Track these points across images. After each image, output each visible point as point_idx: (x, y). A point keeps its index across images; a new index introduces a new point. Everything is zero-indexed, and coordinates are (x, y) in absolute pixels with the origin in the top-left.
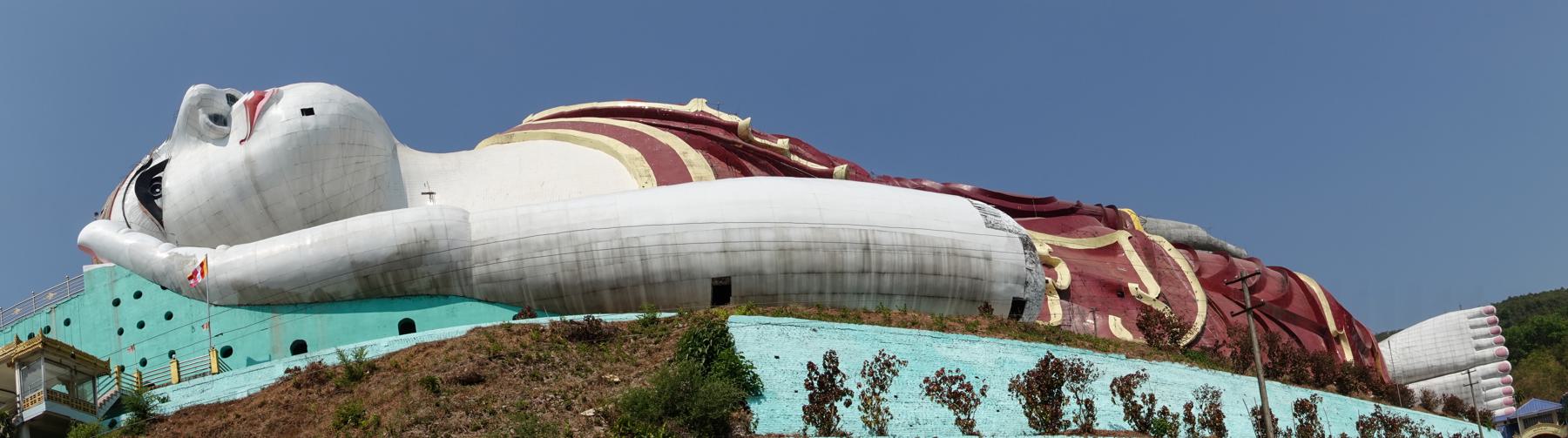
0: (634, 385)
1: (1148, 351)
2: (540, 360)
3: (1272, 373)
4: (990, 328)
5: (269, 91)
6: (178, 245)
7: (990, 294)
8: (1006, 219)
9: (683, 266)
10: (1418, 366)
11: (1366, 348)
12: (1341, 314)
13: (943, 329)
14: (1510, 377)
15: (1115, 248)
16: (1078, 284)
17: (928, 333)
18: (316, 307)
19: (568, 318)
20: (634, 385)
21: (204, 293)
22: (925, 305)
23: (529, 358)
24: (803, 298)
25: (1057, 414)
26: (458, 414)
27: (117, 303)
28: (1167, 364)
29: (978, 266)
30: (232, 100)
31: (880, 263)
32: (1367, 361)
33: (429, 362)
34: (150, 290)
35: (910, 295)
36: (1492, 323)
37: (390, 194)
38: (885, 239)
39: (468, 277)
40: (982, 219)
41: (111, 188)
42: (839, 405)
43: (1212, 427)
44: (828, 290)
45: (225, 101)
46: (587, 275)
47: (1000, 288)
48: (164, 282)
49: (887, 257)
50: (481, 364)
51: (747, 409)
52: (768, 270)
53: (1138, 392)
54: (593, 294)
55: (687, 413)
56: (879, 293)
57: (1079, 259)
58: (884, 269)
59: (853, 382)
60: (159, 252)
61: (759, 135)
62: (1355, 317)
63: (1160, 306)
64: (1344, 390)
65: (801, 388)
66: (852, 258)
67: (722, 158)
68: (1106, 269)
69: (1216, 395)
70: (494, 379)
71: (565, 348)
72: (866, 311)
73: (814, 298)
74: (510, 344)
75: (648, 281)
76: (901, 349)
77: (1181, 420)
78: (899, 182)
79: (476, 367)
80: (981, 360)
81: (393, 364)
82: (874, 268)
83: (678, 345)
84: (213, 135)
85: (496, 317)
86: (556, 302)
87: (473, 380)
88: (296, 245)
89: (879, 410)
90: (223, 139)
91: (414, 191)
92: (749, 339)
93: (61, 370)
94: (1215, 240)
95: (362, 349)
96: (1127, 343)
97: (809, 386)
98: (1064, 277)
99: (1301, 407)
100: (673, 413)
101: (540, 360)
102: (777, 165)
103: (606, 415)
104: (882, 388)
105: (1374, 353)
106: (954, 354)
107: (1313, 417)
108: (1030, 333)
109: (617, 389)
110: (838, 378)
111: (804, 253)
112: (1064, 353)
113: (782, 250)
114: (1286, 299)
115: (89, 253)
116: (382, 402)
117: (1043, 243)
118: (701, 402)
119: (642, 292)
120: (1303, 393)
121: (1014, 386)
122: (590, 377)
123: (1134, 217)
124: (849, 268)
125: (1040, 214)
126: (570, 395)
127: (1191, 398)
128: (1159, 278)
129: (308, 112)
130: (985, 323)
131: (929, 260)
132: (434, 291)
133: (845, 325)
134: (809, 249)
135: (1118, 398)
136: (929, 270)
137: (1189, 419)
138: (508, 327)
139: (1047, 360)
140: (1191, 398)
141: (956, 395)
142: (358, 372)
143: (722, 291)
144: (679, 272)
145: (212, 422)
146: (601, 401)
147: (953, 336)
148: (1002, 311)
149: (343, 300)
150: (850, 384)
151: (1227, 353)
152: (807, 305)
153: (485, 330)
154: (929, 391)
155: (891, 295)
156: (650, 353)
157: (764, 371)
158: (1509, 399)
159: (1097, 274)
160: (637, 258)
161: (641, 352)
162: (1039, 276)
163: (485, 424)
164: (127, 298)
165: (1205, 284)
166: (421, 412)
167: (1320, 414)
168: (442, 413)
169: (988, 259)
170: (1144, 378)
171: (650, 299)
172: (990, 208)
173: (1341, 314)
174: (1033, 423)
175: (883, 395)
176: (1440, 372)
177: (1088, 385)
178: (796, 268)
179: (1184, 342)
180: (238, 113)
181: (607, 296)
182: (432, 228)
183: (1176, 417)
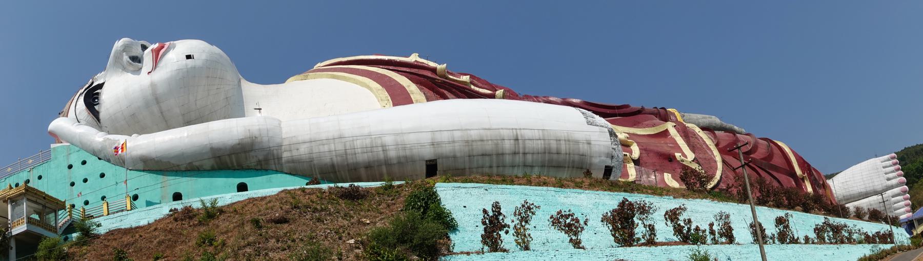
0: (379, 225)
1: (686, 193)
2: (322, 210)
3: (762, 202)
4: (590, 185)
5: (168, 43)
6: (109, 133)
7: (591, 164)
8: (599, 119)
9: (408, 153)
10: (852, 193)
11: (820, 183)
12: (804, 164)
13: (562, 186)
14: (908, 195)
15: (666, 133)
16: (644, 155)
17: (553, 189)
18: (189, 173)
19: (340, 185)
20: (379, 225)
21: (124, 162)
22: (552, 172)
23: (316, 209)
24: (480, 170)
25: (632, 234)
26: (274, 240)
27: (70, 167)
28: (698, 200)
29: (583, 148)
30: (144, 48)
31: (524, 148)
32: (821, 191)
33: (255, 209)
34: (91, 160)
35: (543, 166)
36: (895, 164)
37: (234, 108)
38: (528, 134)
39: (279, 158)
40: (584, 120)
41: (69, 97)
42: (502, 233)
43: (726, 236)
44: (494, 165)
45: (140, 48)
46: (351, 160)
47: (596, 160)
48: (100, 155)
49: (530, 145)
50: (287, 212)
51: (448, 238)
52: (458, 155)
53: (681, 218)
54: (355, 171)
55: (411, 241)
56: (525, 166)
57: (645, 140)
58: (527, 151)
59: (510, 219)
60: (98, 138)
61: (451, 74)
62: (813, 165)
63: (695, 166)
64: (807, 210)
65: (480, 224)
66: (508, 146)
67: (431, 89)
68: (662, 146)
69: (728, 216)
70: (295, 220)
71: (338, 203)
72: (517, 177)
73: (487, 170)
74: (304, 200)
75: (387, 163)
76: (537, 198)
77: (707, 233)
78: (536, 99)
79: (286, 211)
80: (585, 204)
81: (234, 209)
82: (521, 151)
83: (405, 201)
84: (131, 68)
85: (297, 183)
86: (332, 175)
87: (282, 221)
88: (178, 136)
89: (525, 235)
90: (138, 71)
91: (249, 106)
92: (448, 196)
93: (35, 206)
94: (725, 124)
95: (216, 200)
96: (675, 189)
97: (484, 223)
98: (636, 152)
99: (780, 221)
100: (401, 240)
101: (322, 210)
102: (463, 92)
103: (362, 243)
104: (526, 222)
105: (825, 186)
106: (568, 201)
107: (787, 227)
108: (614, 187)
109: (368, 227)
110: (501, 218)
111: (479, 143)
112: (634, 198)
113: (467, 141)
114: (770, 156)
115: (55, 137)
116: (226, 232)
117: (622, 132)
118: (420, 234)
120: (781, 213)
121: (605, 219)
122: (352, 221)
123: (677, 113)
124: (507, 152)
125: (620, 115)
126: (341, 231)
127: (713, 220)
128: (693, 148)
129: (189, 57)
130: (587, 181)
131: (554, 145)
132: (259, 167)
133: (504, 186)
134: (482, 140)
135: (669, 223)
137: (712, 232)
138: (303, 190)
139: (623, 202)
140: (713, 220)
141: (569, 225)
142: (212, 213)
143: (432, 168)
144: (406, 157)
145: (127, 239)
146: (359, 235)
147: (568, 190)
148: (598, 174)
149: (205, 170)
150: (507, 221)
151: (734, 191)
152: (483, 175)
153: (289, 192)
154: (553, 223)
155: (532, 166)
156: (388, 206)
157: (458, 215)
158: (908, 208)
159: (655, 149)
160: (380, 149)
161: (383, 205)
162: (620, 152)
163: (289, 247)
164: (77, 164)
165: (721, 151)
166: (251, 239)
167: (791, 224)
168: (264, 239)
169: (589, 143)
170: (685, 209)
171: (389, 174)
172: (590, 113)
173: (804, 164)
174: (617, 240)
175: (527, 226)
176: (866, 195)
177: (650, 216)
178: (475, 153)
179: (709, 187)
180: (148, 56)
181: (363, 172)
183: (704, 231)
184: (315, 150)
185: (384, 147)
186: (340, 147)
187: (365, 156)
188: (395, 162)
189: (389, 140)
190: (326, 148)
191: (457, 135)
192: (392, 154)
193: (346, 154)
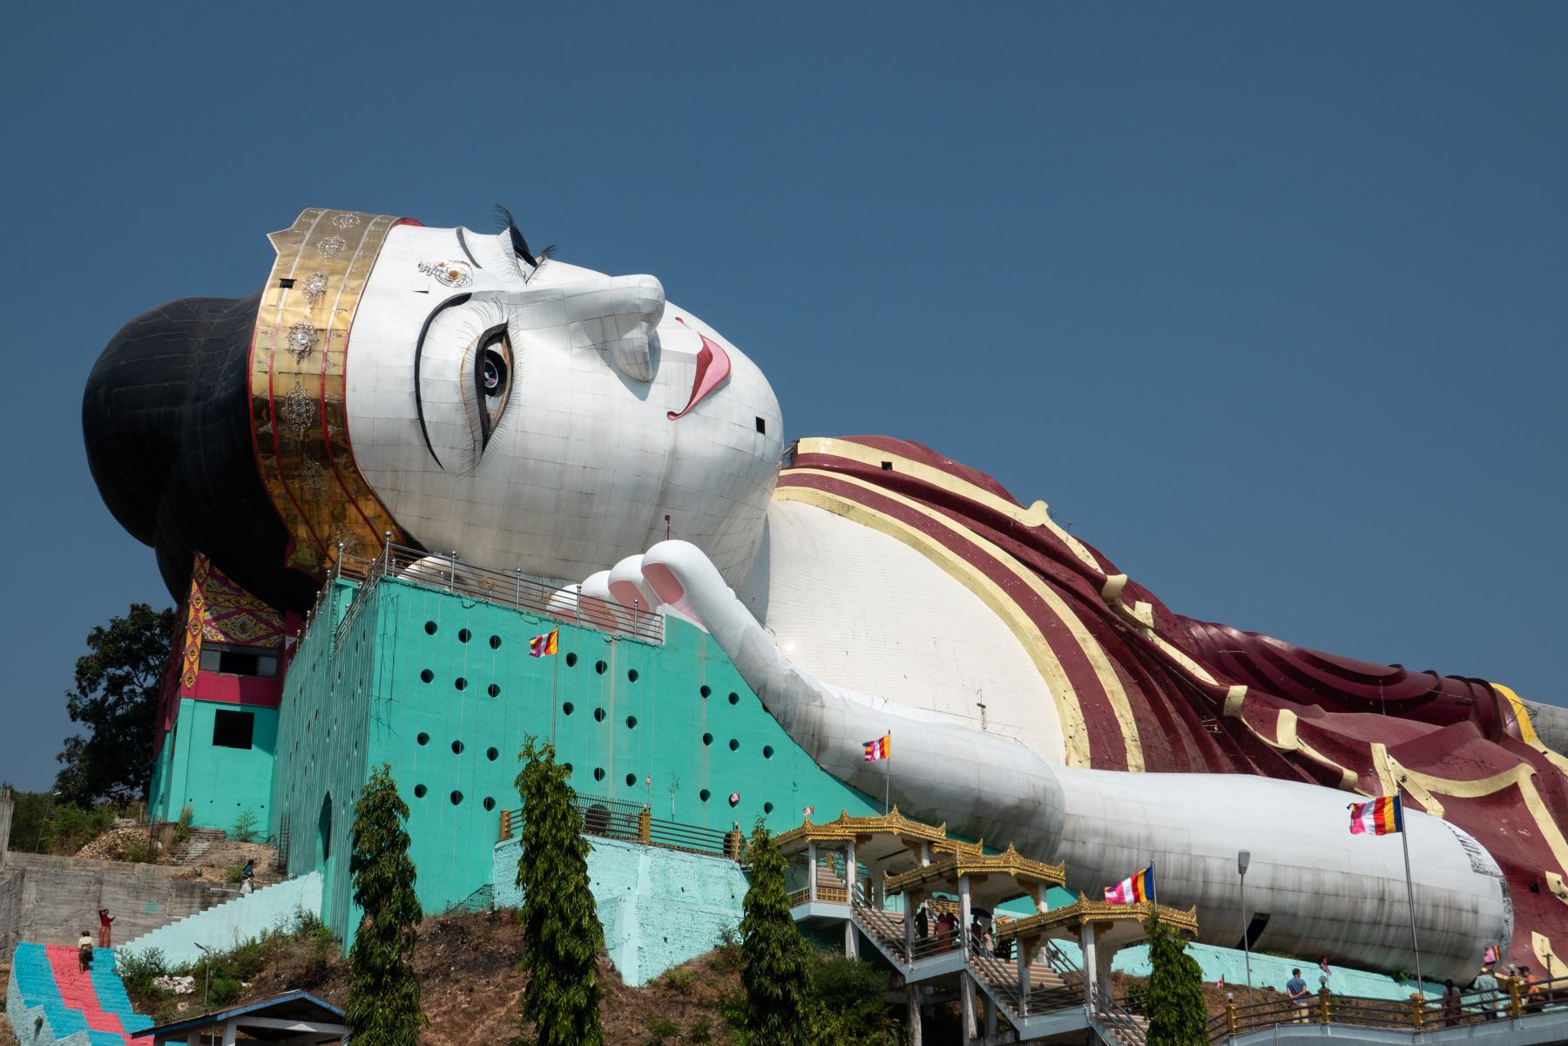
31: (1390, 915)
58: (1393, 921)
82: (1385, 920)
124: (1365, 918)
136: (1427, 925)
144: (1231, 901)
184: (1109, 855)
185: (1206, 873)
188: (1214, 904)
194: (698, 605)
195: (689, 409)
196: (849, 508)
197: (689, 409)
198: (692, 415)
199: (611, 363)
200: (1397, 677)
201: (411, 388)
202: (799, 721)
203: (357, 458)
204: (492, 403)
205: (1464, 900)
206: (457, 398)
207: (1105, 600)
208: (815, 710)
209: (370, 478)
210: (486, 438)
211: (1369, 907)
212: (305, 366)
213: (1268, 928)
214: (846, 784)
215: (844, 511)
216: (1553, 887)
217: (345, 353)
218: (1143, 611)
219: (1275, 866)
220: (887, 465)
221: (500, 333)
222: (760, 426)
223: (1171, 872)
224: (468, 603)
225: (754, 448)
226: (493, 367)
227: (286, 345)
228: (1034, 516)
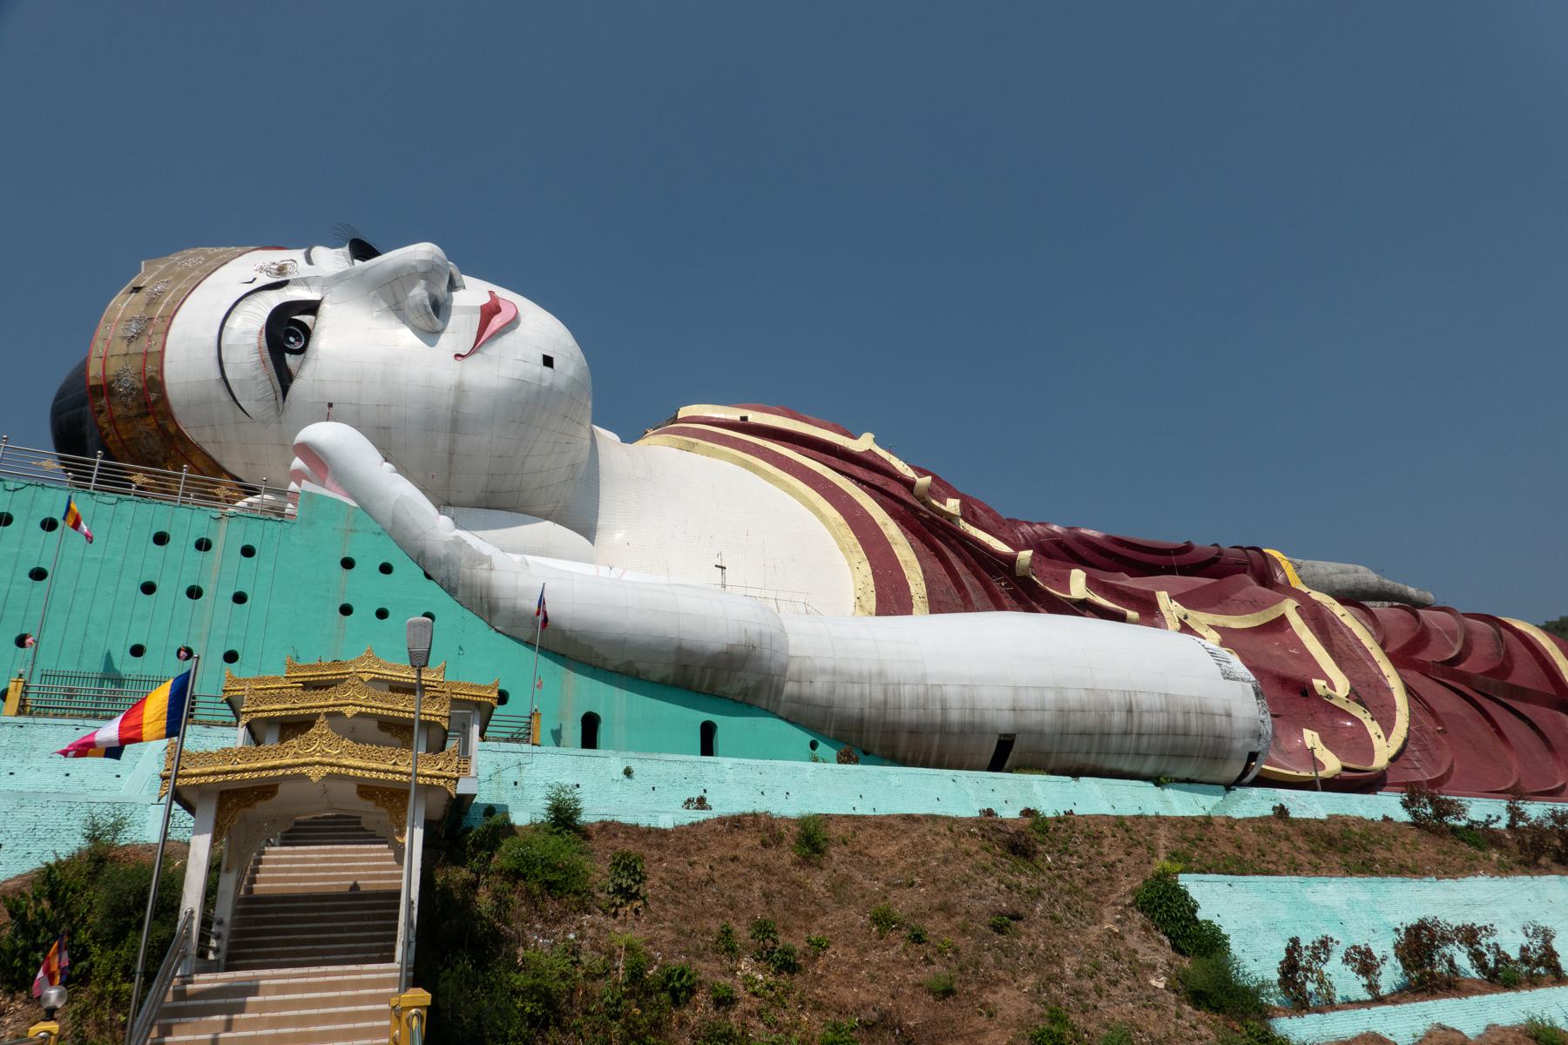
31: (1140, 725)
49: (1146, 718)
52: (1047, 730)
58: (1143, 730)
119: (936, 739)
124: (1115, 730)
131: (1180, 720)
136: (1180, 731)
144: (972, 724)
160: (938, 706)
182: (760, 634)
184: (840, 691)
185: (943, 701)
186: (878, 694)
187: (914, 714)
189: (952, 693)
190: (856, 689)
191: (1050, 696)
192: (955, 716)
193: (885, 702)
194: (346, 482)
195: (473, 351)
196: (694, 444)
197: (473, 351)
198: (477, 356)
199: (405, 320)
200: (1188, 548)
201: (214, 354)
202: (464, 586)
203: (178, 418)
204: (291, 360)
205: (1216, 704)
206: (256, 358)
207: (918, 498)
208: (481, 573)
209: (191, 434)
210: (285, 390)
211: (1118, 719)
212: (133, 348)
213: (1015, 748)
214: (529, 644)
215: (690, 448)
216: (1320, 691)
217: (166, 333)
218: (953, 505)
219: (1016, 688)
220: (744, 419)
221: (312, 308)
222: (548, 361)
223: (907, 702)
224: (11, 486)
225: (541, 379)
226: (288, 331)
227: (120, 333)
228: (863, 444)
